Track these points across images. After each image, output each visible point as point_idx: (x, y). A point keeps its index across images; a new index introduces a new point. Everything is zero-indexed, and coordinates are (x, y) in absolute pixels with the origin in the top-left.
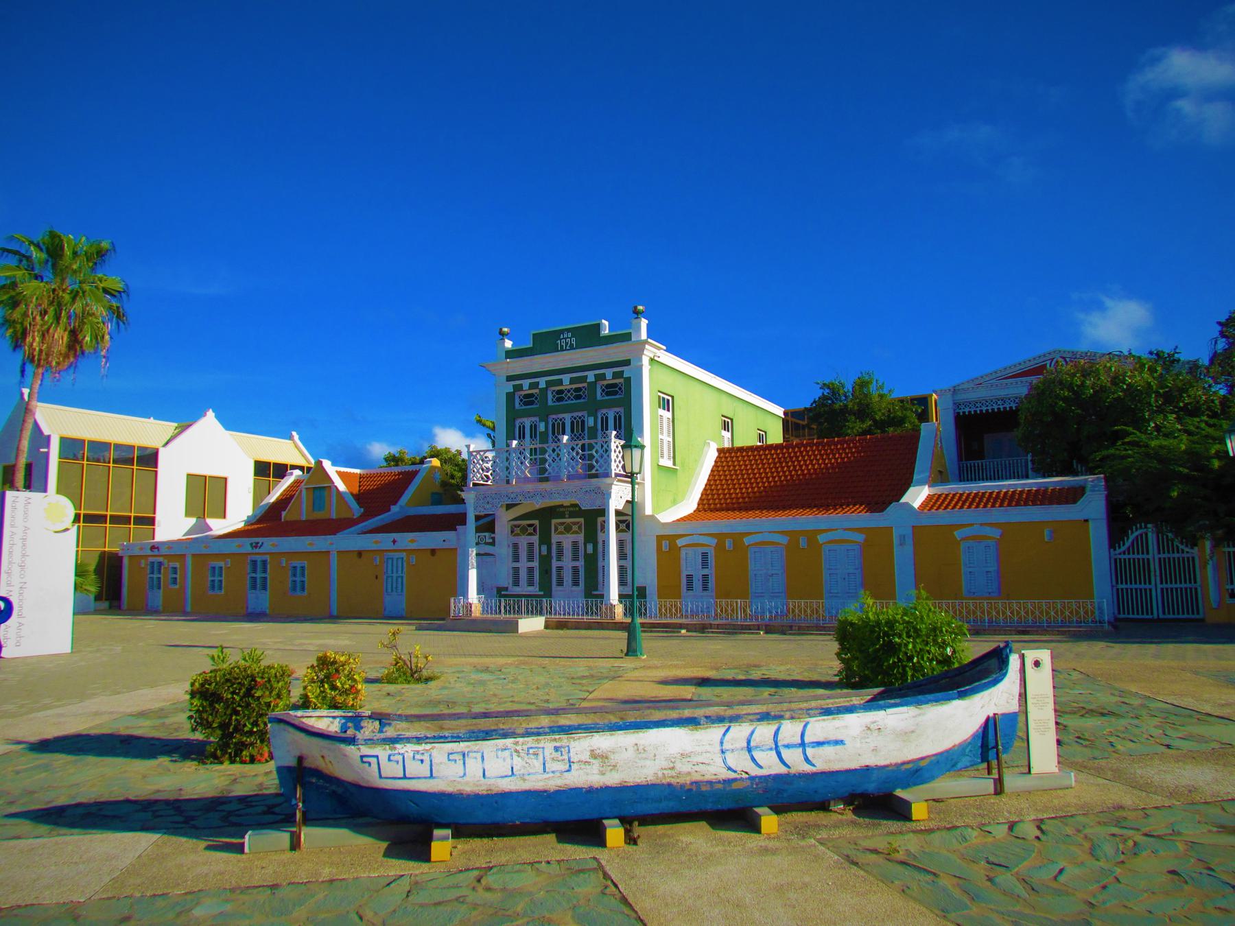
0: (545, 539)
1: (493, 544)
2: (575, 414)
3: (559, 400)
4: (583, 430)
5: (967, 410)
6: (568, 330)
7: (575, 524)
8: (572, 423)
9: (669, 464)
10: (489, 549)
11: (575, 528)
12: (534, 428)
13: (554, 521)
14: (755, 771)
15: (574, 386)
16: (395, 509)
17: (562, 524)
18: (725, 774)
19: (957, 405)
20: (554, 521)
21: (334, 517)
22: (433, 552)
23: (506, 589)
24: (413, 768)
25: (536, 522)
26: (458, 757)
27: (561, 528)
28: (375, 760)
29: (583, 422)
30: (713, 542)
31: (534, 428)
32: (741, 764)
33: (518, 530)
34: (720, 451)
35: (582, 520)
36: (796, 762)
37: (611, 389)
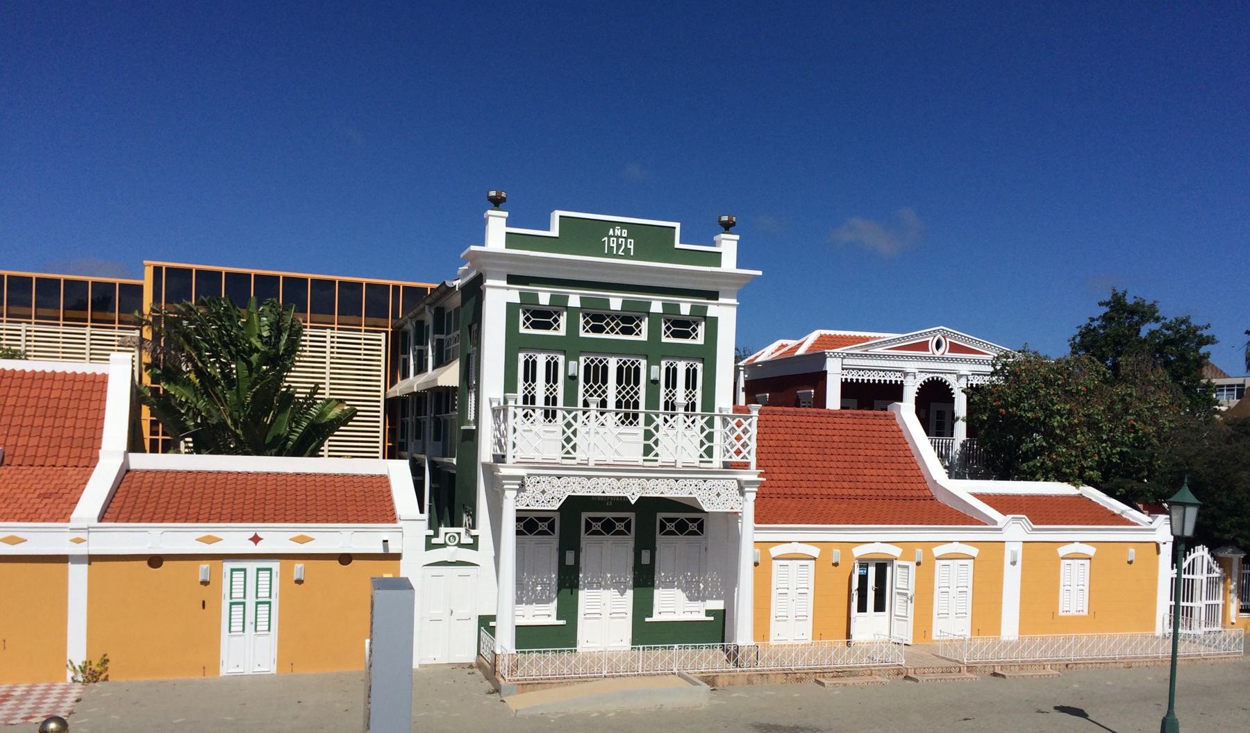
1: (474, 546)
6: (623, 225)
8: (620, 369)
10: (466, 555)
11: (620, 526)
13: (585, 516)
29: (637, 370)
37: (683, 327)
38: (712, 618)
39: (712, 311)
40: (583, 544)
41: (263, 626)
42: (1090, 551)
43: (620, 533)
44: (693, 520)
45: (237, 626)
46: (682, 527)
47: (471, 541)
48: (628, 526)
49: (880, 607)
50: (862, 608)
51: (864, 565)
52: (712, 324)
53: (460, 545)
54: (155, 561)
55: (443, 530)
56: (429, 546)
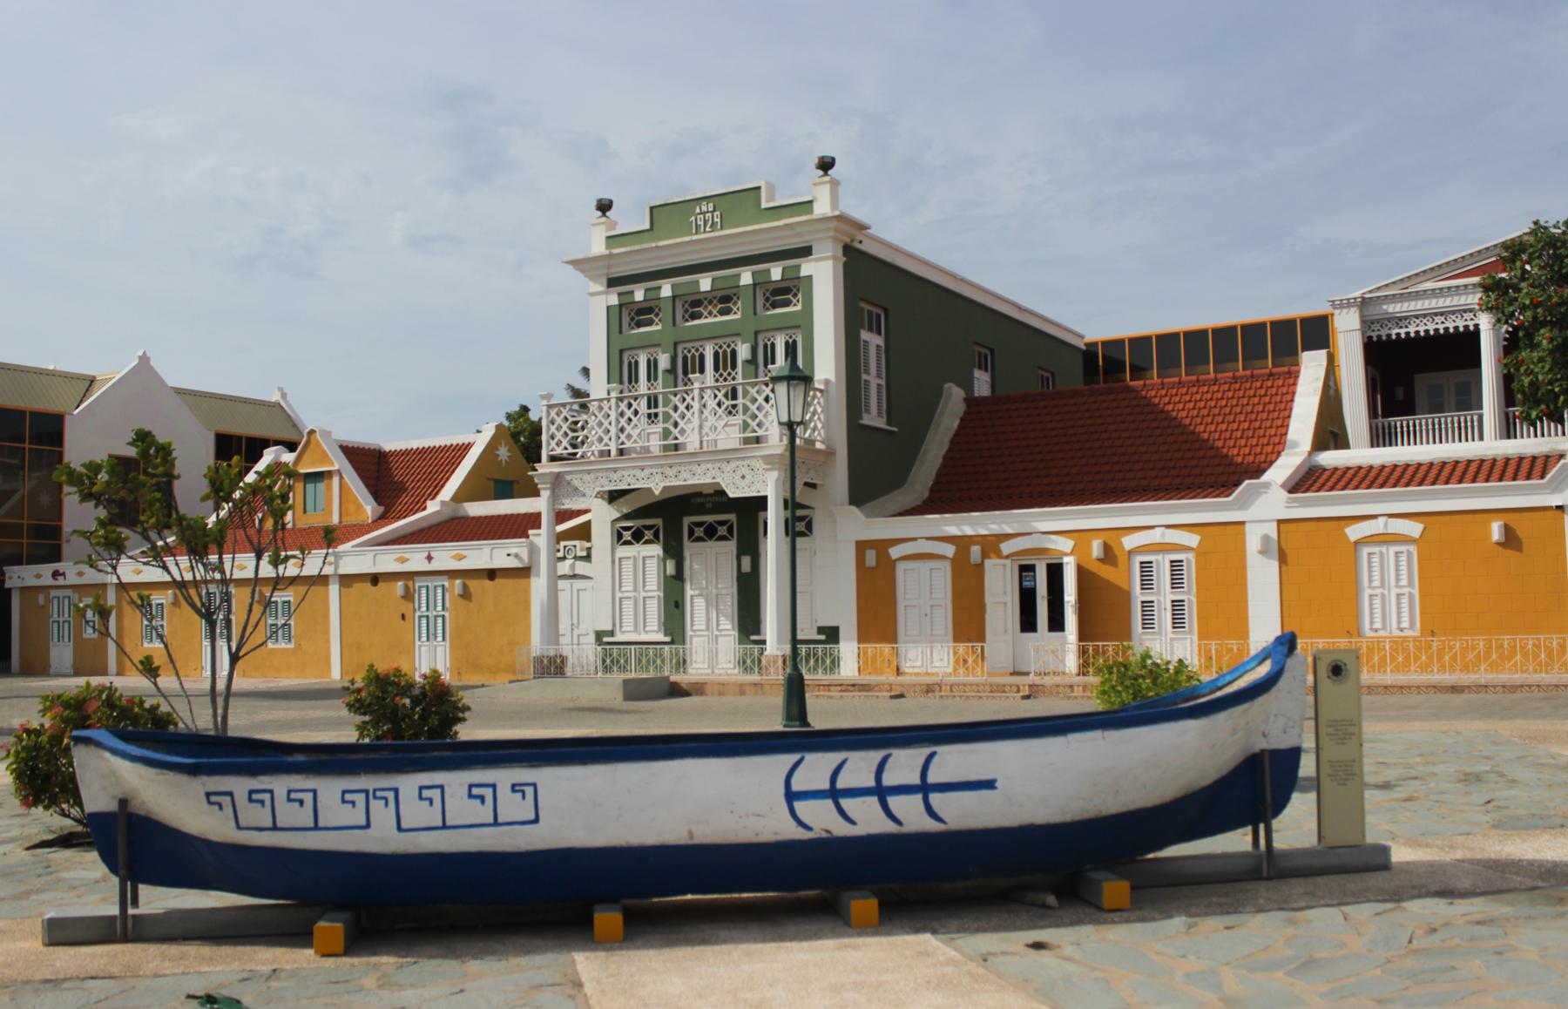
0: (674, 551)
1: (588, 558)
2: (720, 341)
3: (694, 316)
4: (734, 366)
5: (1384, 333)
7: (722, 523)
8: (716, 355)
9: (881, 423)
10: (581, 568)
11: (722, 531)
12: (652, 365)
13: (687, 521)
14: (841, 829)
15: (719, 294)
16: (433, 507)
18: (793, 832)
19: (1366, 323)
20: (687, 521)
21: (335, 520)
22: (492, 574)
23: (612, 633)
24: (290, 814)
25: (658, 522)
26: (360, 799)
27: (699, 532)
28: (228, 799)
29: (734, 353)
30: (949, 550)
31: (652, 365)
32: (821, 819)
33: (627, 536)
34: (971, 402)
35: (732, 517)
36: (911, 814)
38: (823, 637)
39: (807, 268)
40: (687, 554)
42: (1414, 529)
43: (722, 538)
49: (1057, 624)
50: (1028, 624)
51: (1027, 569)
53: (576, 558)
54: (375, 579)
55: (563, 544)
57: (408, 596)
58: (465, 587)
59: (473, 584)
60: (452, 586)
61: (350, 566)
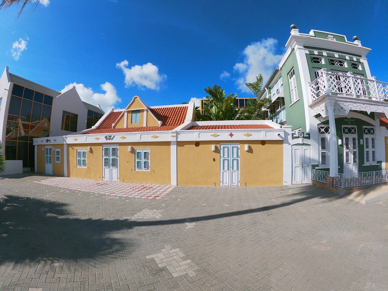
7: (353, 128)
10: (306, 141)
11: (353, 131)
17: (346, 128)
20: (343, 126)
22: (263, 142)
27: (346, 131)
33: (323, 130)
41: (235, 168)
43: (353, 133)
44: (372, 129)
45: (226, 168)
46: (369, 131)
47: (308, 136)
48: (355, 131)
52: (362, 64)
54: (197, 144)
56: (293, 138)
57: (217, 151)
58: (250, 147)
59: (253, 146)
60: (243, 148)
61: (181, 138)
